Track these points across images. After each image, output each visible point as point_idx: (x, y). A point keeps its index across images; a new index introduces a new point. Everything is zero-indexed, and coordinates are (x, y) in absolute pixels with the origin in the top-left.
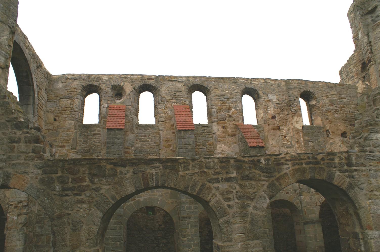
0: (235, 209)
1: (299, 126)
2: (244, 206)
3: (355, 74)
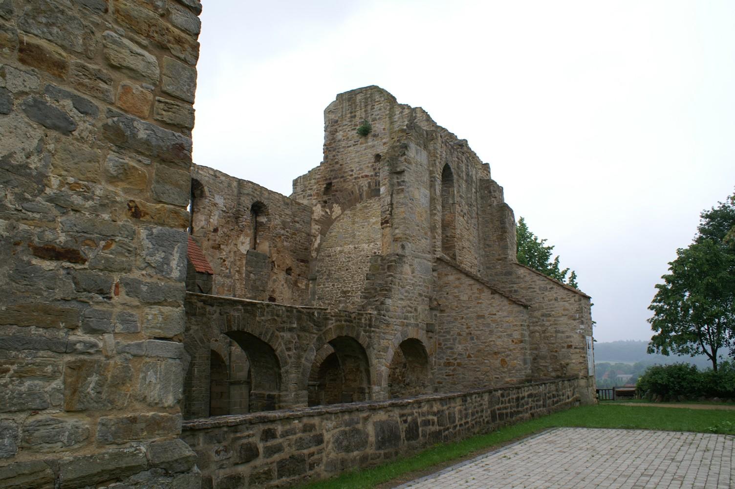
0: (293, 360)
2: (299, 357)
3: (314, 193)
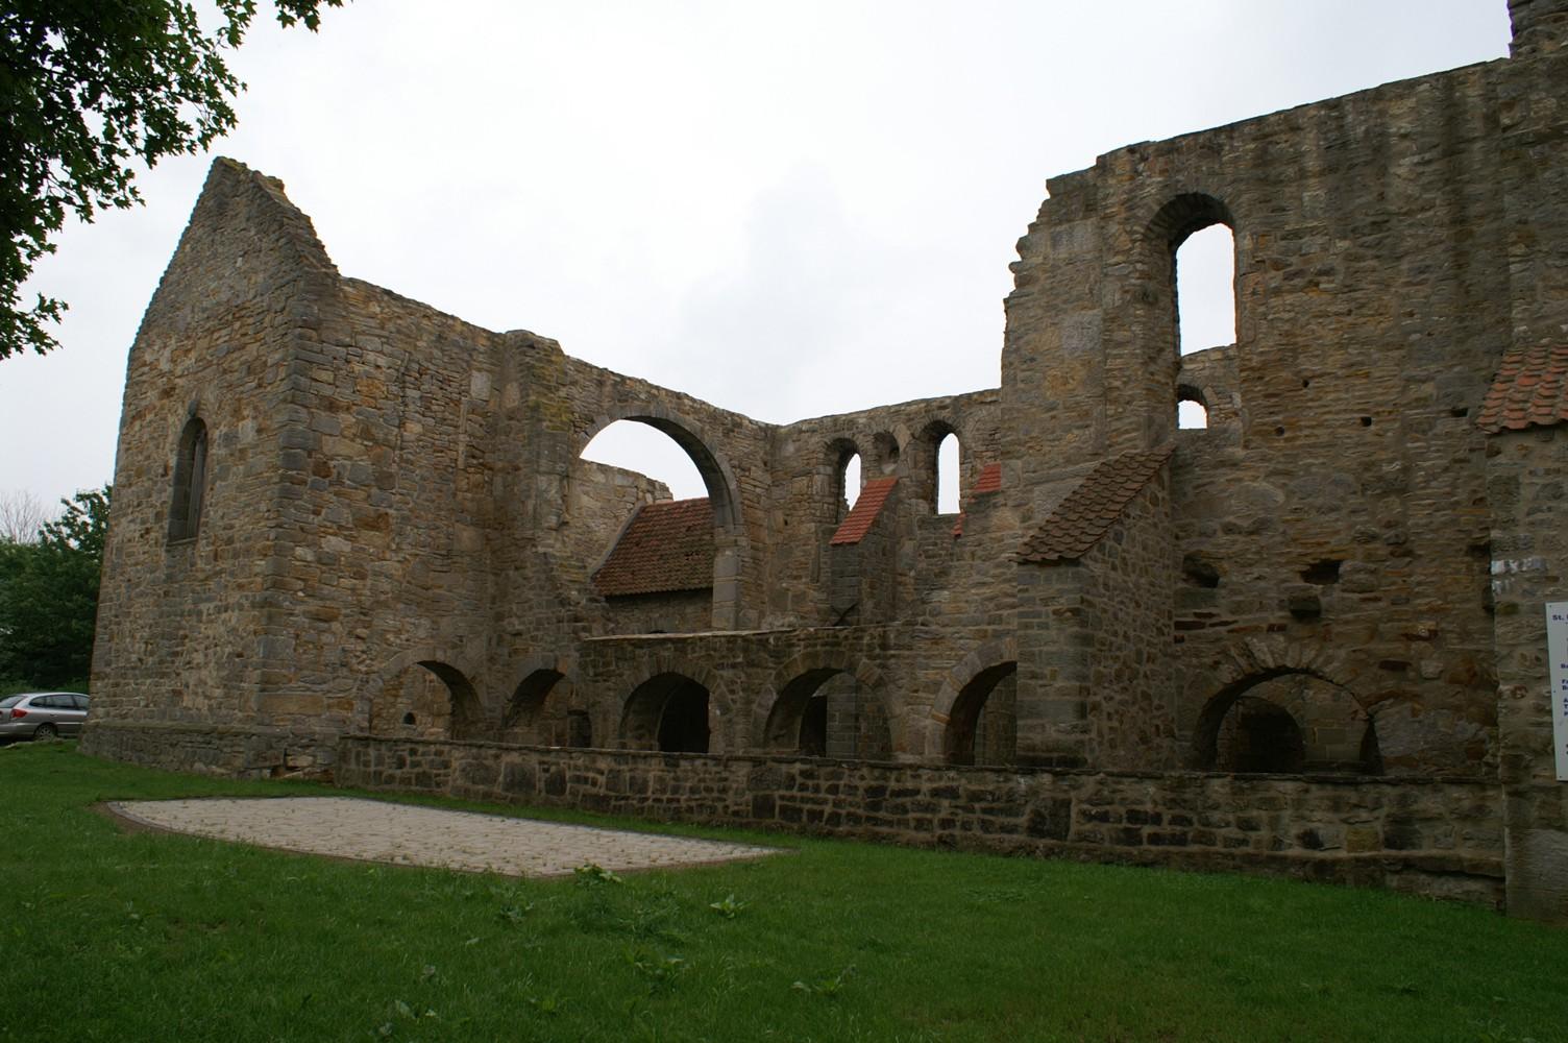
0: (739, 705)
2: (749, 702)
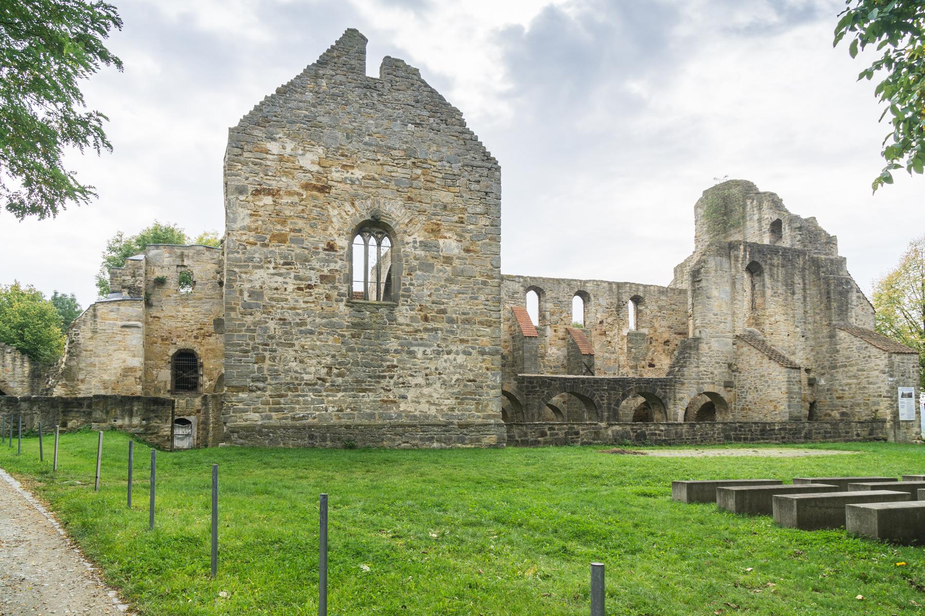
1: (625, 332)
